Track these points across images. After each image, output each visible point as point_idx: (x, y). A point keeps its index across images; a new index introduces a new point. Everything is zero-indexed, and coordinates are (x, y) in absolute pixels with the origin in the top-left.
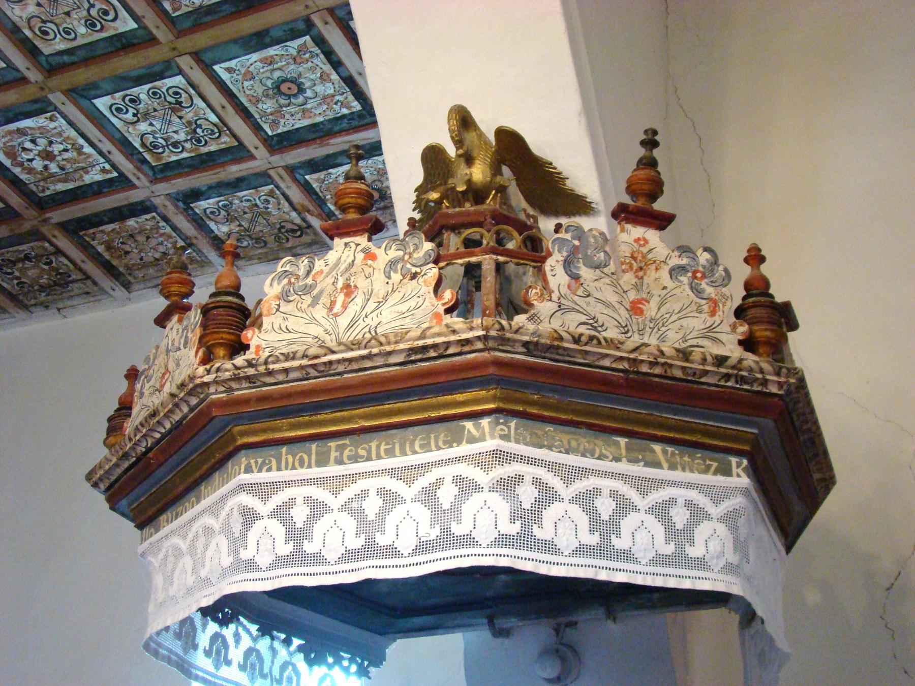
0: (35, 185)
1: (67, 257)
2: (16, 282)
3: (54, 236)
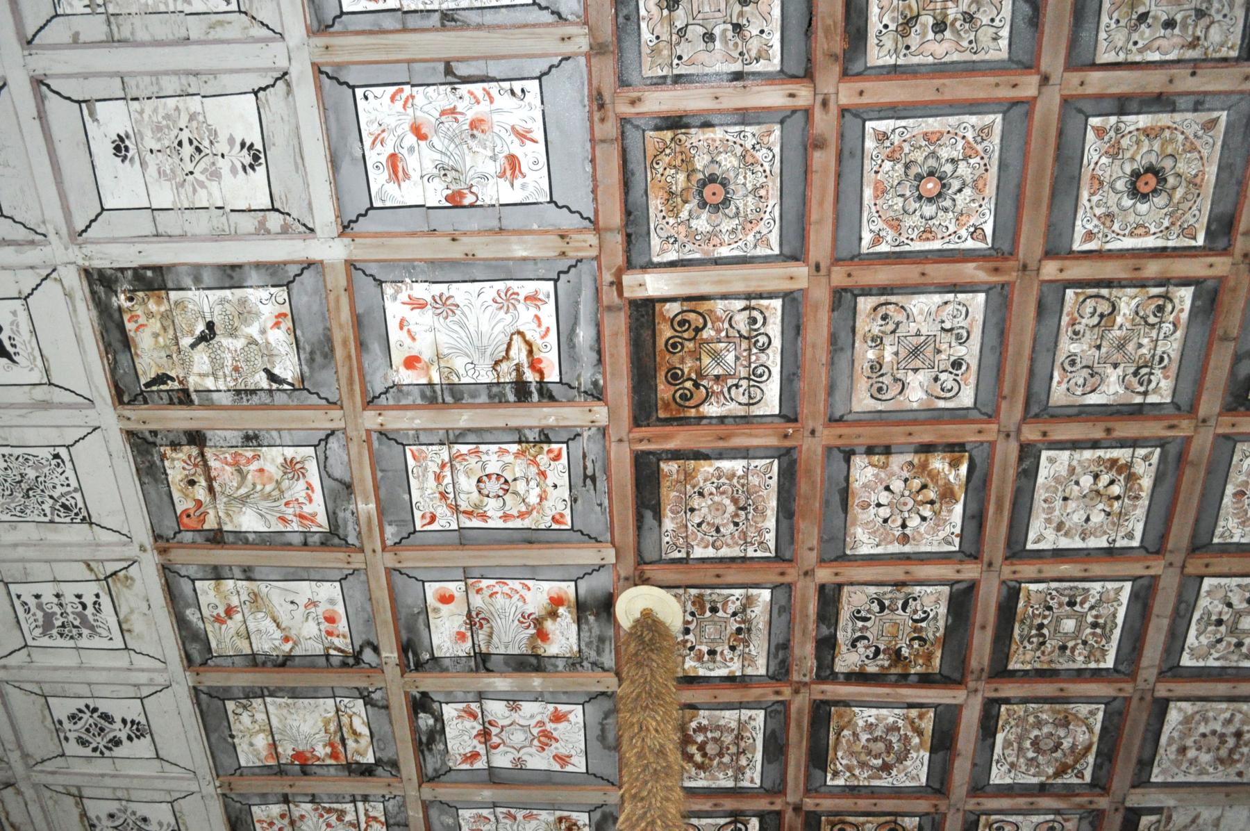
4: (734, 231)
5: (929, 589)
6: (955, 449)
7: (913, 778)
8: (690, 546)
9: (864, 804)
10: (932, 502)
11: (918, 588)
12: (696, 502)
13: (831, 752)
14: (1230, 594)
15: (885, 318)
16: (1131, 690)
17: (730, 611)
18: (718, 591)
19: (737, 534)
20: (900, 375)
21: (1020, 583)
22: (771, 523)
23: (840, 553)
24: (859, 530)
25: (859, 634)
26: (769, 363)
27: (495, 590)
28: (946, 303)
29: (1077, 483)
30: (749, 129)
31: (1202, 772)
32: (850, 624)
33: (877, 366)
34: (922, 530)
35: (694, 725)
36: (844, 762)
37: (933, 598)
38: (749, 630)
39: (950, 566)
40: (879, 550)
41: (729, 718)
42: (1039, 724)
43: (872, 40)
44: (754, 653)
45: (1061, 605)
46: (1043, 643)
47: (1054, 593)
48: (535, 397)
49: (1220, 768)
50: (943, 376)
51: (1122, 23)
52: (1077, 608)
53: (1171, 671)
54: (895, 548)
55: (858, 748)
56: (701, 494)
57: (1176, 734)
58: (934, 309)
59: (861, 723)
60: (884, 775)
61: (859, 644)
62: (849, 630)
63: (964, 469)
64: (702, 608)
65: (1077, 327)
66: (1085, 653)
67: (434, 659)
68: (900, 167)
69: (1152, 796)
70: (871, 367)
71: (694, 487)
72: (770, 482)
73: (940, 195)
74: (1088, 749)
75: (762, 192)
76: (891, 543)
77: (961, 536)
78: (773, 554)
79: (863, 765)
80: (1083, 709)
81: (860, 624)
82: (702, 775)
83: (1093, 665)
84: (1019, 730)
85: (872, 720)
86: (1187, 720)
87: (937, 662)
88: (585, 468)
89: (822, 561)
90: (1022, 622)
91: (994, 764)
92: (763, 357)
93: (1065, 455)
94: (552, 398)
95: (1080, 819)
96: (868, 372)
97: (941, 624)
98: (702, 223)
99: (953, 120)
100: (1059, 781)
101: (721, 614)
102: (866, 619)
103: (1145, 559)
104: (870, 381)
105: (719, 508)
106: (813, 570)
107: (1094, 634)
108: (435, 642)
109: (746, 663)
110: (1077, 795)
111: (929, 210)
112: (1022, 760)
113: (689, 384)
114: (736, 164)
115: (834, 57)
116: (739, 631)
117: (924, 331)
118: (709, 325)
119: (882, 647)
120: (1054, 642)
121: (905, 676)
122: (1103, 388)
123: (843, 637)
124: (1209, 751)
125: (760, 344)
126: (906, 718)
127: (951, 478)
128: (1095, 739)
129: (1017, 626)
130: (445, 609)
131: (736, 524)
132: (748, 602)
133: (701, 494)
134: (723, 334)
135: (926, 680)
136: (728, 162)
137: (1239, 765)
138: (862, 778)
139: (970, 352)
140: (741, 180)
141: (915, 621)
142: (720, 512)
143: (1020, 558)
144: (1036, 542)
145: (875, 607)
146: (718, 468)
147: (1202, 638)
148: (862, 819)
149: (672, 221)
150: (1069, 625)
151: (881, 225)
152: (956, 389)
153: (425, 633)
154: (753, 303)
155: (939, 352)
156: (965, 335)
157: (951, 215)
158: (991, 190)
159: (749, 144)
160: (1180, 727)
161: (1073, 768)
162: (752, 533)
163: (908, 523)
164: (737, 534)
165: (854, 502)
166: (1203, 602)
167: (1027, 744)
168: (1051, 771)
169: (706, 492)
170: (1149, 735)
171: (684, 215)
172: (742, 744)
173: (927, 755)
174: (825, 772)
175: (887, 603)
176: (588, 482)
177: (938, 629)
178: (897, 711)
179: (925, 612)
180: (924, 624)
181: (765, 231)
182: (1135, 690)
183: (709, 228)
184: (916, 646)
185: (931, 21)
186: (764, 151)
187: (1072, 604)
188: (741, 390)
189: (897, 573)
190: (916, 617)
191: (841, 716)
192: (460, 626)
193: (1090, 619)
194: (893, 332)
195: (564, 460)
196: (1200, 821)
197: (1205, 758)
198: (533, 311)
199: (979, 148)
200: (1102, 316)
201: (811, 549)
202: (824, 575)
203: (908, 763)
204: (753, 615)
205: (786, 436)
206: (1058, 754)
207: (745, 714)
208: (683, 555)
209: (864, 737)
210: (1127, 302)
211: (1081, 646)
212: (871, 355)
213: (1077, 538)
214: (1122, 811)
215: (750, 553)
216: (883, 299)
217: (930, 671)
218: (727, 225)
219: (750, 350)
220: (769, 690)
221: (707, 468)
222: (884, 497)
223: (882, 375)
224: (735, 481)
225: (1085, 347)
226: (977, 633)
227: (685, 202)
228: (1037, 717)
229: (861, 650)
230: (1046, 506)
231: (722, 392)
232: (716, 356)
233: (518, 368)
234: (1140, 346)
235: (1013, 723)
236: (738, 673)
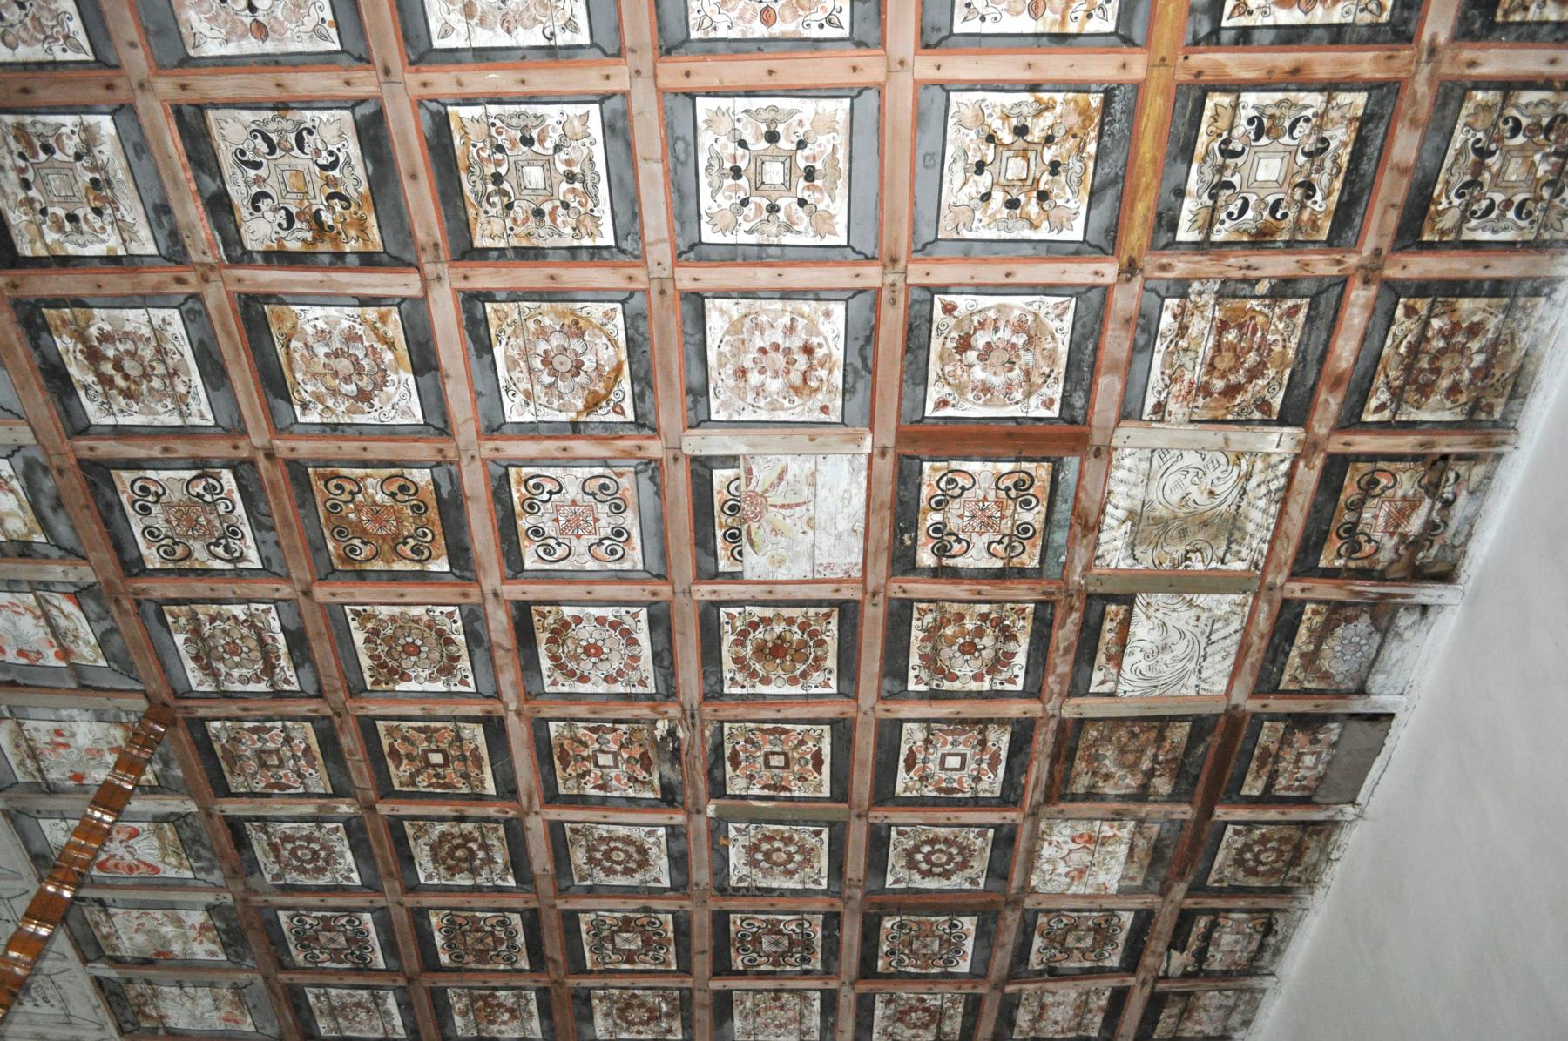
0: (1362, 10)
1: (1529, 84)
2: (1511, 214)
3: (1472, 64)
5: (324, 115)
7: (404, 413)
9: (350, 448)
11: (308, 114)
13: (287, 373)
14: (738, 125)
16: (644, 279)
17: (71, 152)
19: (28, 21)
21: (445, 105)
23: (181, 56)
24: (192, 15)
25: (255, 189)
31: (774, 407)
35: (93, 331)
36: (309, 388)
38: (109, 182)
39: (334, 75)
40: (231, 49)
41: (135, 319)
42: (543, 333)
44: (129, 219)
45: (513, 142)
46: (509, 206)
47: (498, 123)
49: (798, 401)
52: (537, 147)
53: (693, 251)
54: (251, 46)
55: (320, 369)
57: (725, 349)
59: (309, 330)
60: (365, 407)
62: (241, 182)
66: (572, 222)
69: (714, 438)
74: (618, 370)
76: (244, 36)
79: (334, 392)
80: (596, 311)
81: (252, 173)
82: (136, 408)
83: (587, 242)
84: (520, 341)
85: (321, 324)
86: (735, 328)
87: (374, 233)
89: (160, 68)
90: (468, 169)
91: (503, 392)
95: (636, 473)
97: (359, 171)
100: (593, 418)
101: (58, 155)
102: (257, 165)
103: (602, 64)
107: (573, 191)
109: (126, 236)
110: (621, 437)
112: (538, 388)
116: (94, 182)
119: (294, 211)
120: (524, 204)
121: (339, 256)
123: (238, 194)
124: (776, 375)
126: (364, 322)
128: (624, 356)
129: (463, 176)
132: (90, 140)
135: (368, 261)
137: (820, 396)
138: (341, 413)
141: (323, 167)
143: (430, 63)
144: (444, 36)
147: (719, 197)
148: (359, 472)
150: (534, 175)
160: (727, 338)
161: (606, 397)
162: (48, 22)
164: (28, 21)
166: (705, 139)
167: (537, 363)
168: (580, 404)
170: (692, 350)
172: (170, 362)
173: (411, 378)
174: (290, 402)
175: (275, 138)
177: (359, 182)
178: (347, 310)
179: (331, 153)
180: (336, 173)
182: (650, 280)
184: (338, 208)
187: (527, 141)
189: (262, 85)
190: (321, 161)
191: (280, 318)
193: (562, 168)
196: (789, 477)
197: (775, 385)
203: (390, 389)
206: (582, 379)
207: (158, 314)
209: (321, 350)
211: (561, 211)
213: (498, 28)
214: (682, 461)
215: (60, 56)
217: (371, 248)
220: (166, 277)
228: (537, 322)
235: (509, 331)
236: (121, 252)
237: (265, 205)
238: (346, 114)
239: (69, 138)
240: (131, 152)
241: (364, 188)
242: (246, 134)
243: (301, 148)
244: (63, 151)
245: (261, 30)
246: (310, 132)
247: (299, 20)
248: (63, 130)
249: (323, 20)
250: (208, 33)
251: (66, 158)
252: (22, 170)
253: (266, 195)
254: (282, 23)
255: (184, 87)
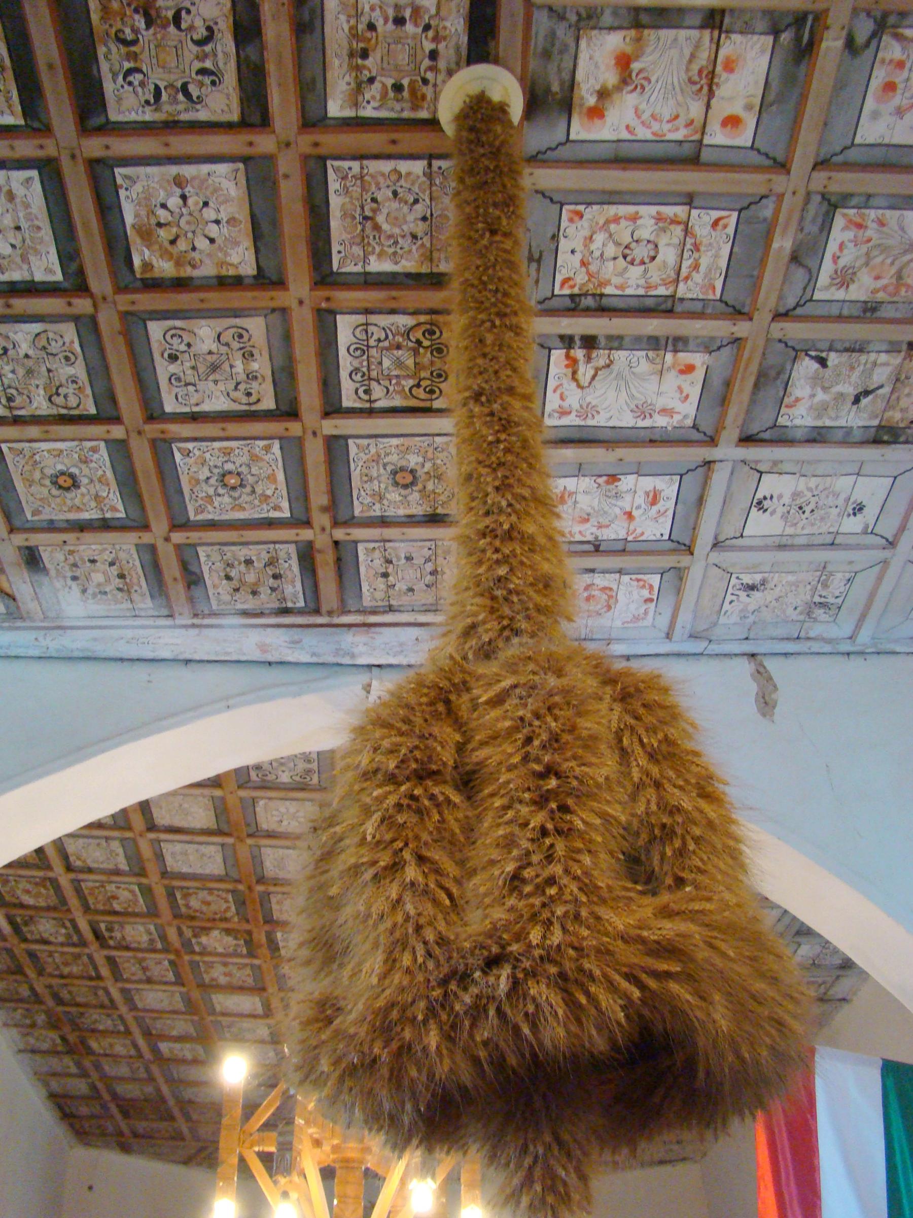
4: (387, 454)
5: (133, 117)
6: (153, 285)
8: (429, 175)
10: (160, 225)
12: (420, 228)
15: (249, 394)
17: (377, 85)
18: (392, 115)
19: (373, 188)
20: (224, 350)
22: (335, 202)
25: (208, 48)
26: (350, 359)
27: (670, 126)
28: (197, 405)
29: (13, 246)
30: (378, 513)
32: (221, 65)
33: (248, 356)
34: (162, 193)
37: (126, 104)
38: (351, 55)
40: (205, 168)
43: (294, 557)
48: (577, 339)
50: (183, 347)
51: (124, 562)
54: (188, 171)
56: (414, 237)
58: (207, 400)
61: (205, 33)
62: (220, 55)
63: (137, 262)
64: (413, 91)
65: (75, 386)
67: (776, 32)
68: (259, 490)
70: (252, 355)
71: (423, 245)
72: (341, 248)
73: (224, 475)
75: (365, 479)
76: (194, 178)
77: (116, 188)
78: (329, 163)
81: (208, 64)
88: (538, 270)
89: (270, 158)
92: (356, 363)
93: (39, 277)
94: (562, 337)
96: (255, 352)
97: (104, 66)
98: (413, 460)
99: (225, 517)
101: (390, 82)
102: (203, 72)
104: (251, 343)
105: (395, 221)
106: (279, 148)
108: (765, 61)
111: (229, 467)
113: (426, 343)
114: (387, 495)
115: (319, 551)
116: (365, 54)
117: (211, 384)
118: (407, 389)
119: (172, 29)
122: (30, 338)
123: (226, 43)
125: (359, 375)
127: (147, 252)
130: (737, 109)
131: (374, 200)
133: (414, 237)
134: (394, 382)
136: (394, 495)
139: (164, 370)
140: (383, 486)
141: (138, 70)
142: (393, 215)
144: (29, 180)
145: (193, 90)
146: (396, 263)
149: (439, 462)
151: (266, 458)
152: (168, 337)
153: (775, 74)
154: (367, 405)
155: (193, 368)
156: (173, 381)
157: (211, 464)
158: (184, 480)
159: (377, 506)
162: (356, 190)
163: (181, 202)
164: (373, 188)
165: (246, 225)
169: (409, 239)
171: (428, 465)
175: (181, 97)
176: (536, 256)
177: (106, 57)
179: (130, 84)
180: (127, 65)
181: (362, 455)
183: (407, 456)
185: (255, 564)
186: (366, 502)
188: (375, 337)
189: (181, 144)
190: (139, 77)
192: (727, 80)
194: (238, 384)
195: (559, 278)
198: (565, 404)
199: (200, 502)
200: (58, 394)
201: (286, 176)
202: (265, 143)
204: (347, 78)
205: (328, 299)
208: (436, 163)
210: (41, 405)
212: (255, 366)
215: (355, 165)
216: (254, 408)
218: (394, 458)
219: (369, 370)
221: (408, 265)
222: (213, 231)
223: (241, 349)
224: (378, 249)
225: (61, 371)
226: (58, 62)
227: (427, 473)
229: (199, 23)
230: (36, 223)
231: (394, 336)
232: (399, 364)
233: (589, 359)
234: (13, 372)
237: (201, 32)
238: (114, 116)
239: (373, 98)
240: (319, 85)
241: (101, 50)
242: (208, 100)
243: (157, 89)
244: (384, 85)
245: (179, 182)
246: (147, 102)
247: (146, 190)
248: (376, 104)
249: (127, 189)
250: (223, 180)
251: (384, 79)
252: (430, 69)
253: (199, 43)
254: (161, 187)
255: (251, 144)
